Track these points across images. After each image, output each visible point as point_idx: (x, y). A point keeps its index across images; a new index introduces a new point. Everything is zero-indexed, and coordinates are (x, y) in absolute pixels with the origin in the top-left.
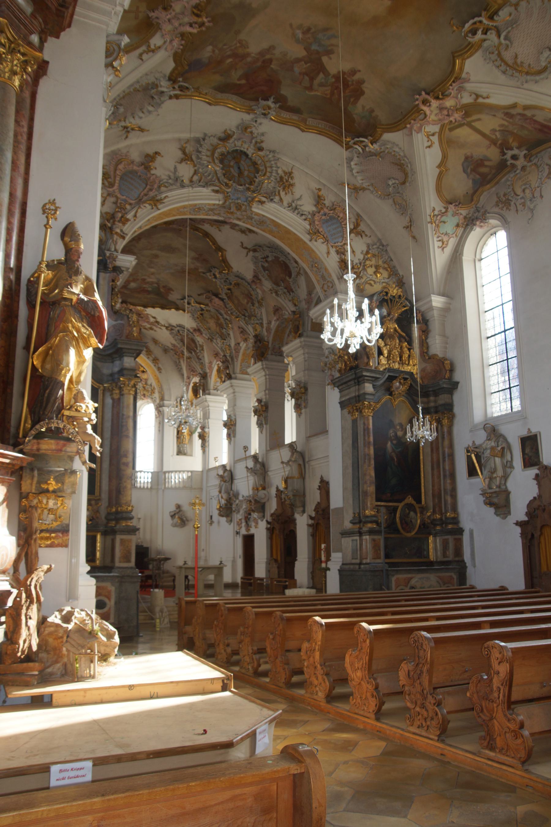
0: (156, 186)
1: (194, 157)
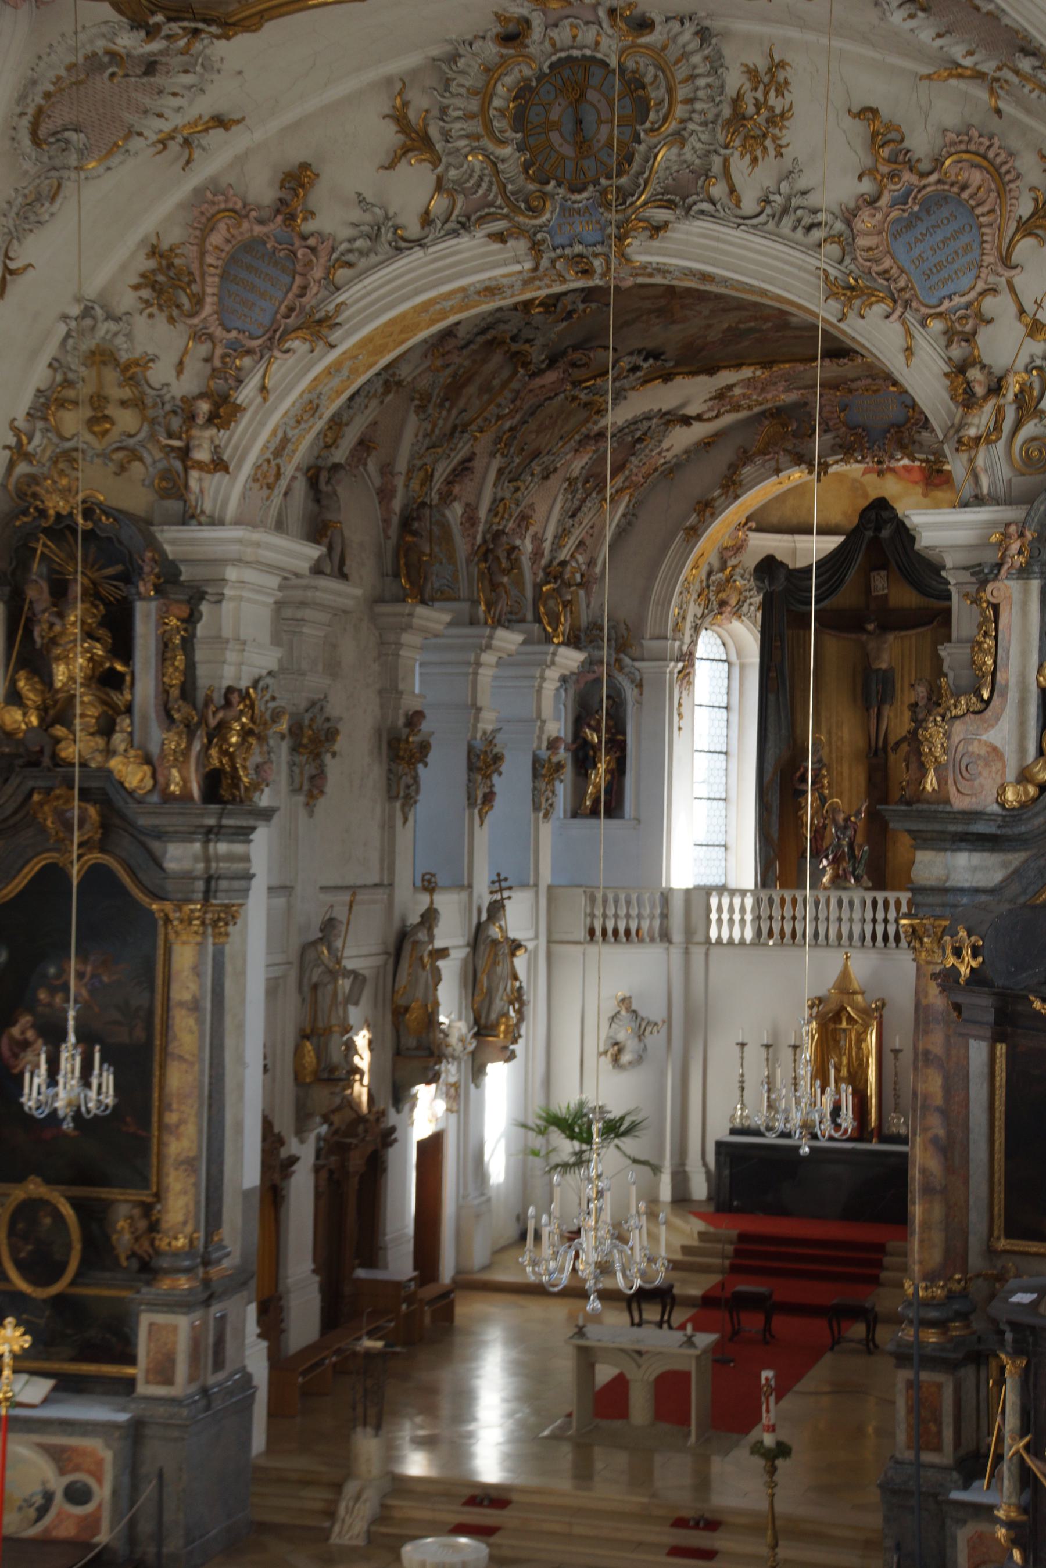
0: (318, 273)
1: (434, 132)
